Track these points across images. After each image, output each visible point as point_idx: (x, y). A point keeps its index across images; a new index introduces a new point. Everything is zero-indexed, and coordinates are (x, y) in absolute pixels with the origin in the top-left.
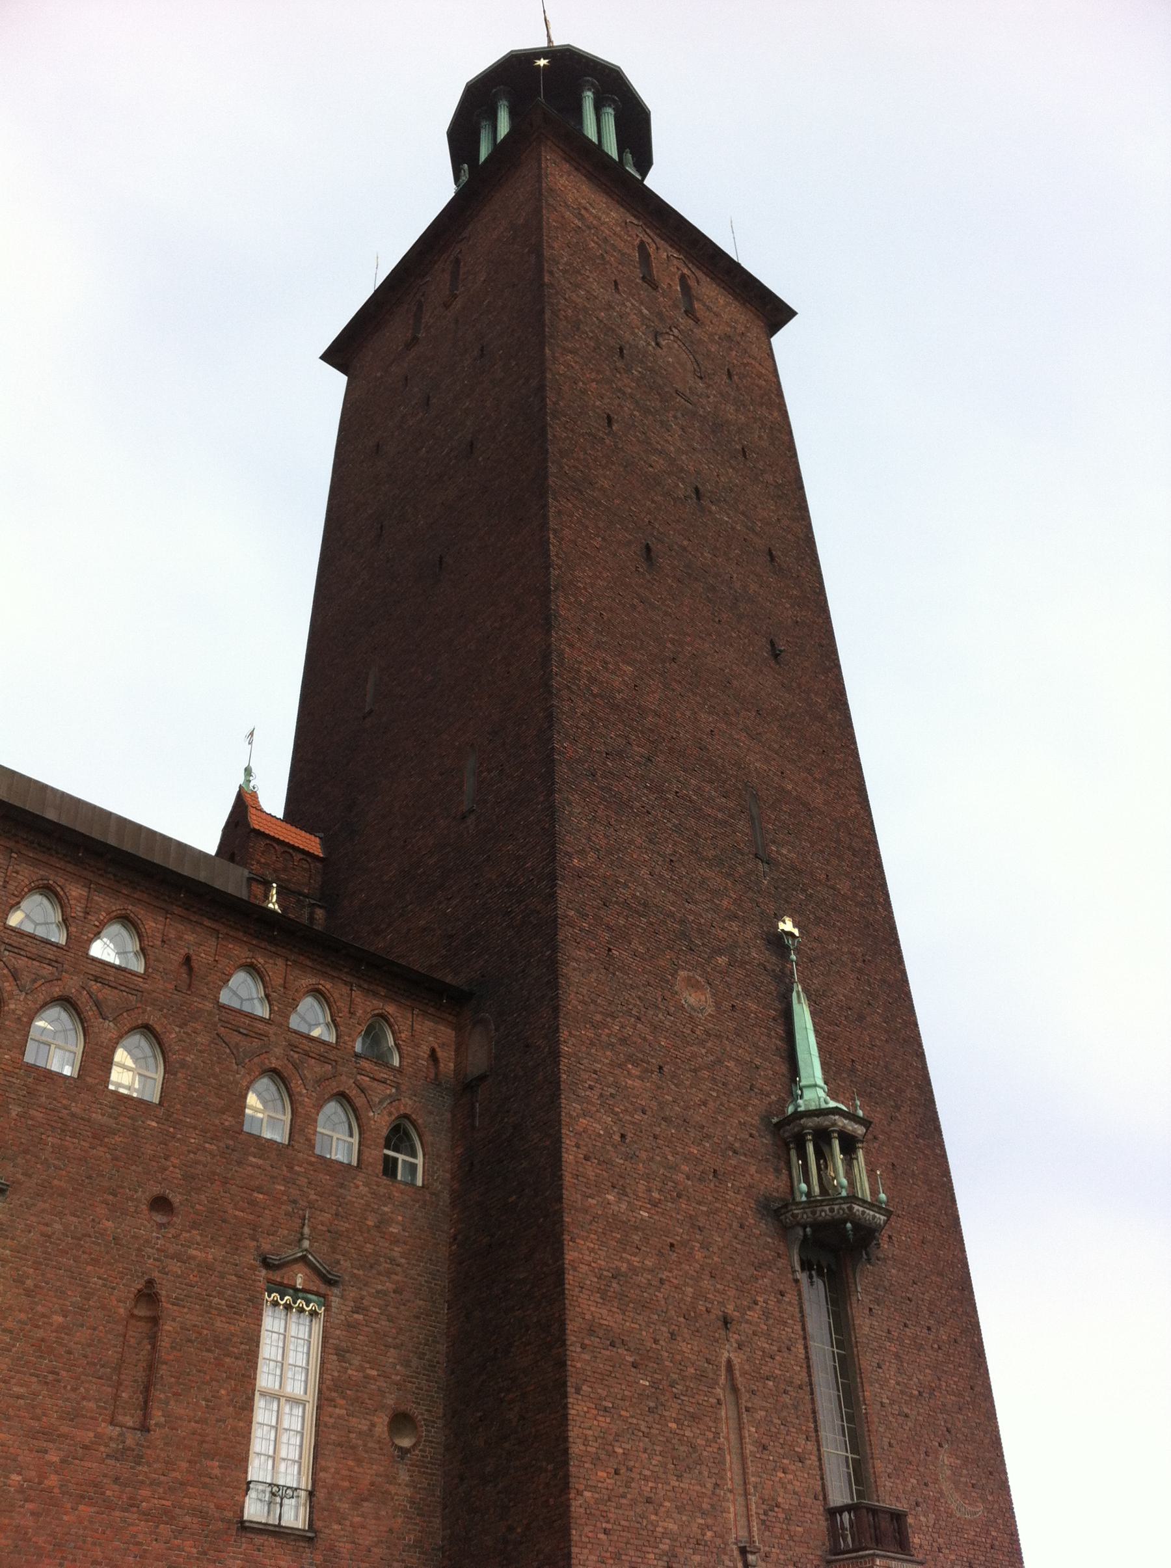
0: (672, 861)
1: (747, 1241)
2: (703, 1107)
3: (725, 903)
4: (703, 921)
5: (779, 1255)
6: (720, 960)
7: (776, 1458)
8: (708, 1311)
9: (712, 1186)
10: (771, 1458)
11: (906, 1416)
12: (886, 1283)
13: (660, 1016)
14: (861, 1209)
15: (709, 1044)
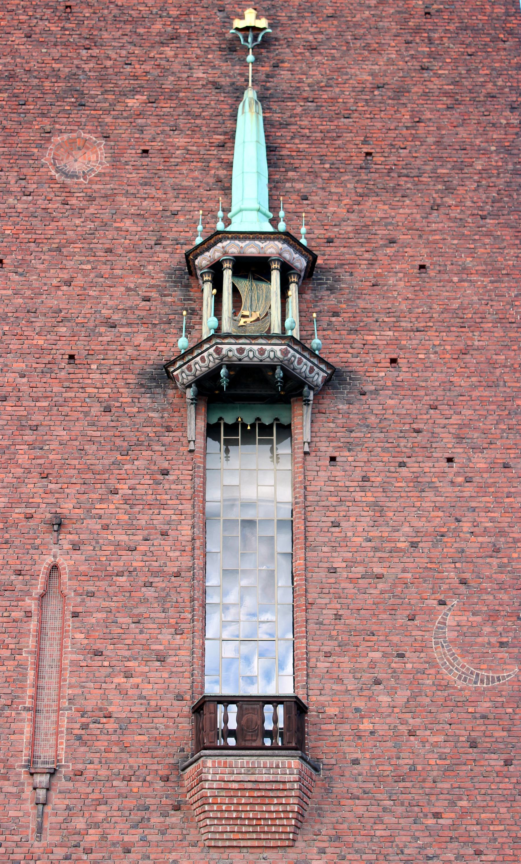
0: (70, 7)
1: (113, 424)
2: (65, 288)
3: (158, 26)
4: (109, 63)
5: (169, 429)
6: (131, 102)
7: (113, 663)
8: (29, 517)
9: (63, 374)
10: (106, 663)
11: (379, 577)
12: (373, 420)
13: (11, 200)
14: (234, 347)
15: (92, 210)
